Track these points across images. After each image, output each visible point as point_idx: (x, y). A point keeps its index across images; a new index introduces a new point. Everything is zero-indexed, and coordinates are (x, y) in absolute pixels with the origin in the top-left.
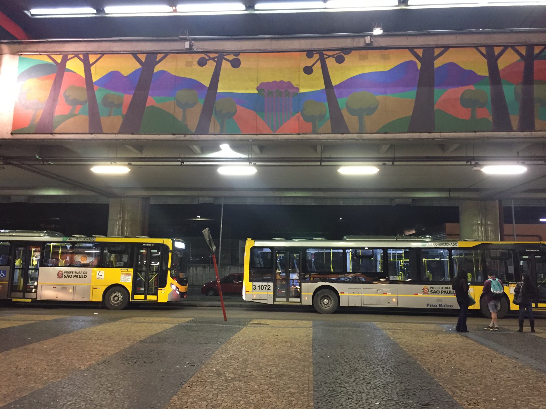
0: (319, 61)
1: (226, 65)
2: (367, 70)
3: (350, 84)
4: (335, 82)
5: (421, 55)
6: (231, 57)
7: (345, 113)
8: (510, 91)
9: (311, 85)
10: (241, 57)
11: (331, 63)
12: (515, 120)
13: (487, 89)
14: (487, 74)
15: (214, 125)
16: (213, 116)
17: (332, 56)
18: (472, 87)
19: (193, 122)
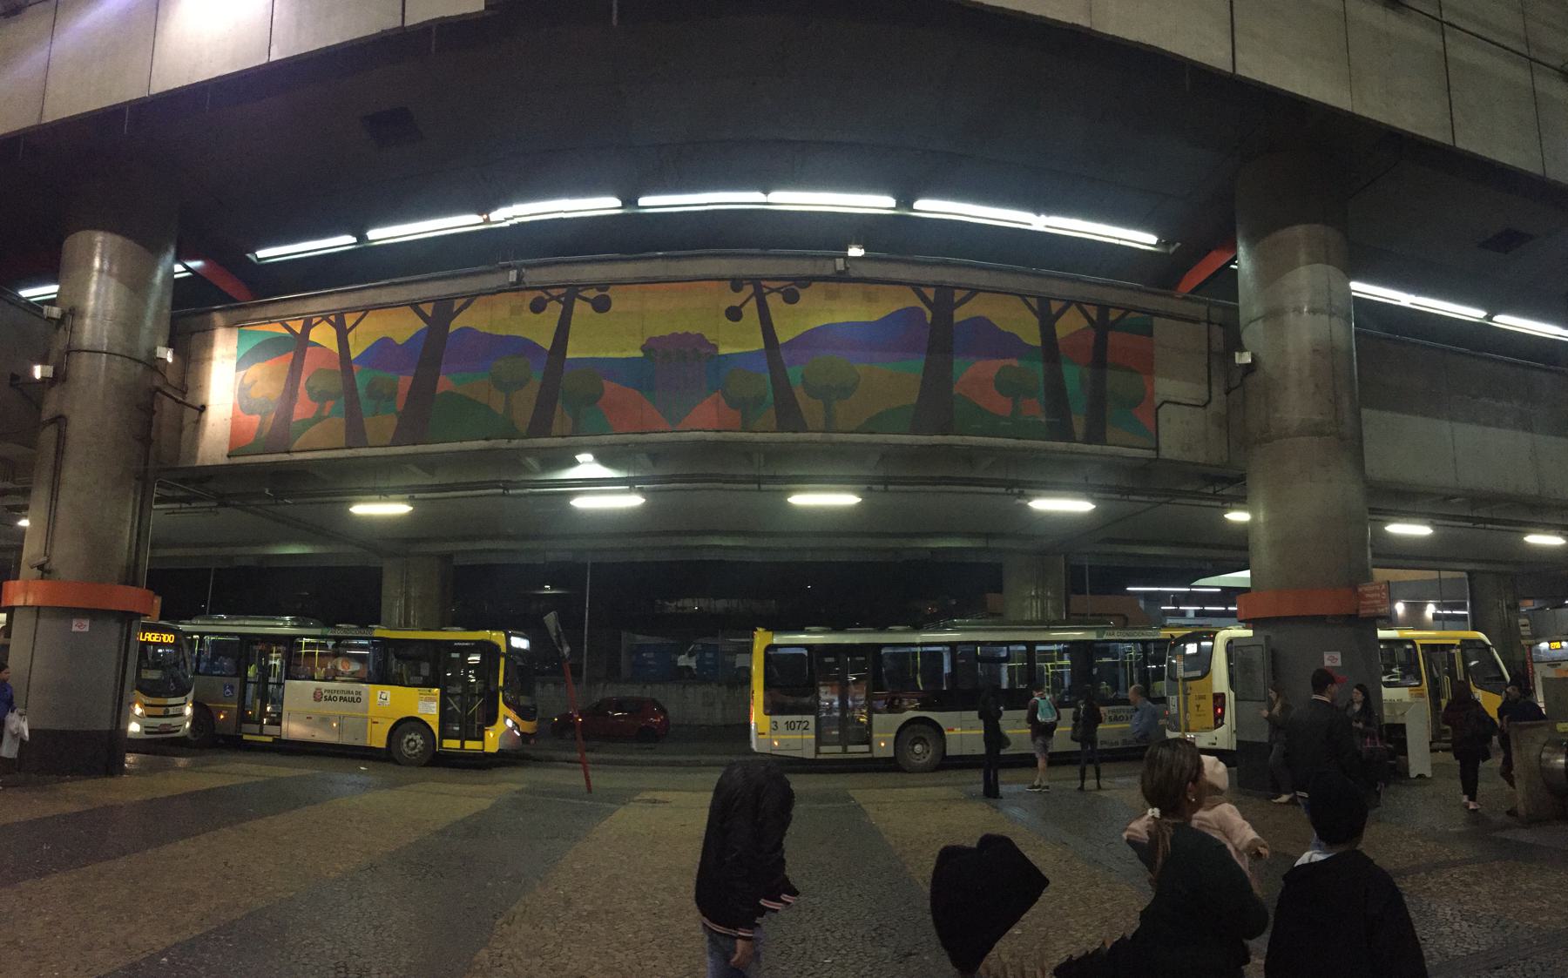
0: (754, 300)
1: (581, 309)
2: (840, 318)
3: (807, 341)
4: (783, 336)
5: (932, 298)
6: (592, 294)
7: (800, 395)
8: (1073, 376)
9: (739, 341)
10: (612, 293)
11: (774, 302)
12: (1079, 424)
13: (1039, 369)
14: (1039, 343)
15: (562, 417)
16: (559, 404)
17: (777, 290)
18: (1015, 363)
19: (524, 413)
